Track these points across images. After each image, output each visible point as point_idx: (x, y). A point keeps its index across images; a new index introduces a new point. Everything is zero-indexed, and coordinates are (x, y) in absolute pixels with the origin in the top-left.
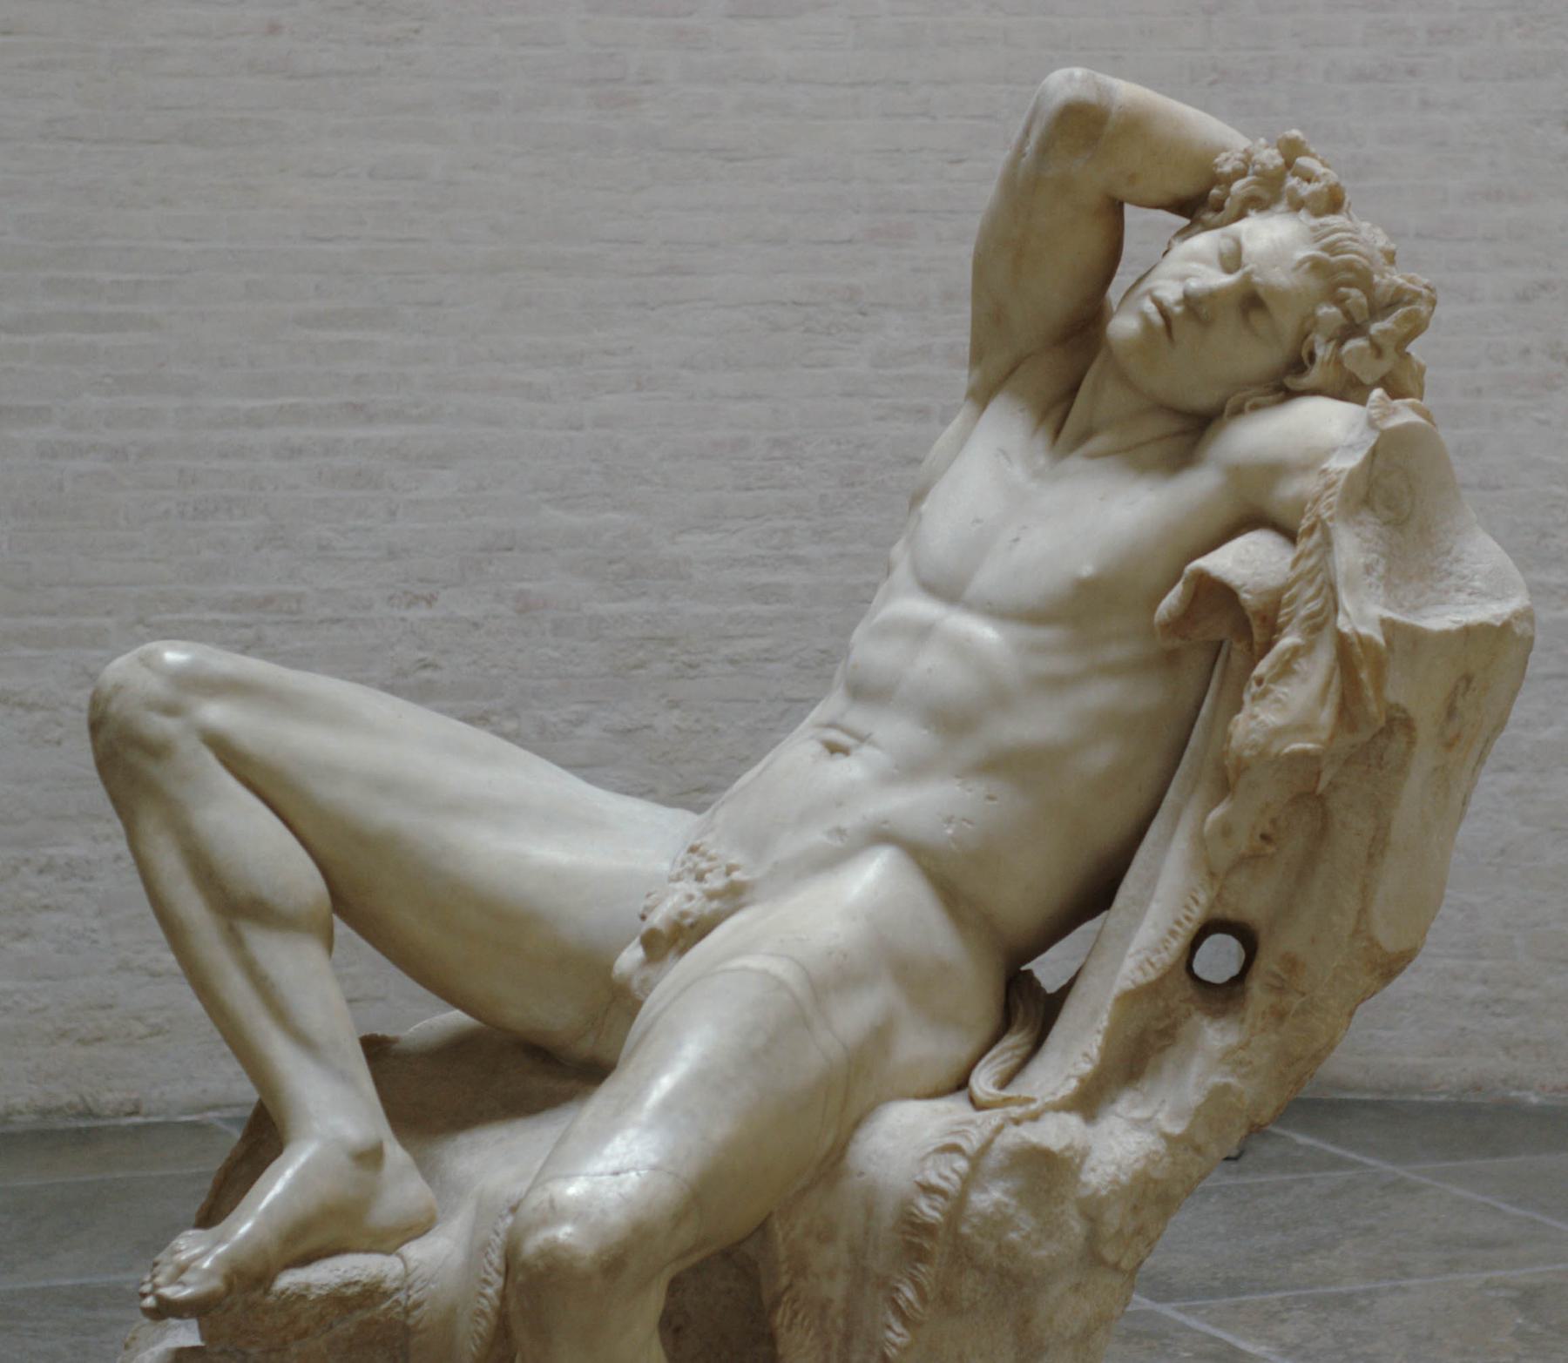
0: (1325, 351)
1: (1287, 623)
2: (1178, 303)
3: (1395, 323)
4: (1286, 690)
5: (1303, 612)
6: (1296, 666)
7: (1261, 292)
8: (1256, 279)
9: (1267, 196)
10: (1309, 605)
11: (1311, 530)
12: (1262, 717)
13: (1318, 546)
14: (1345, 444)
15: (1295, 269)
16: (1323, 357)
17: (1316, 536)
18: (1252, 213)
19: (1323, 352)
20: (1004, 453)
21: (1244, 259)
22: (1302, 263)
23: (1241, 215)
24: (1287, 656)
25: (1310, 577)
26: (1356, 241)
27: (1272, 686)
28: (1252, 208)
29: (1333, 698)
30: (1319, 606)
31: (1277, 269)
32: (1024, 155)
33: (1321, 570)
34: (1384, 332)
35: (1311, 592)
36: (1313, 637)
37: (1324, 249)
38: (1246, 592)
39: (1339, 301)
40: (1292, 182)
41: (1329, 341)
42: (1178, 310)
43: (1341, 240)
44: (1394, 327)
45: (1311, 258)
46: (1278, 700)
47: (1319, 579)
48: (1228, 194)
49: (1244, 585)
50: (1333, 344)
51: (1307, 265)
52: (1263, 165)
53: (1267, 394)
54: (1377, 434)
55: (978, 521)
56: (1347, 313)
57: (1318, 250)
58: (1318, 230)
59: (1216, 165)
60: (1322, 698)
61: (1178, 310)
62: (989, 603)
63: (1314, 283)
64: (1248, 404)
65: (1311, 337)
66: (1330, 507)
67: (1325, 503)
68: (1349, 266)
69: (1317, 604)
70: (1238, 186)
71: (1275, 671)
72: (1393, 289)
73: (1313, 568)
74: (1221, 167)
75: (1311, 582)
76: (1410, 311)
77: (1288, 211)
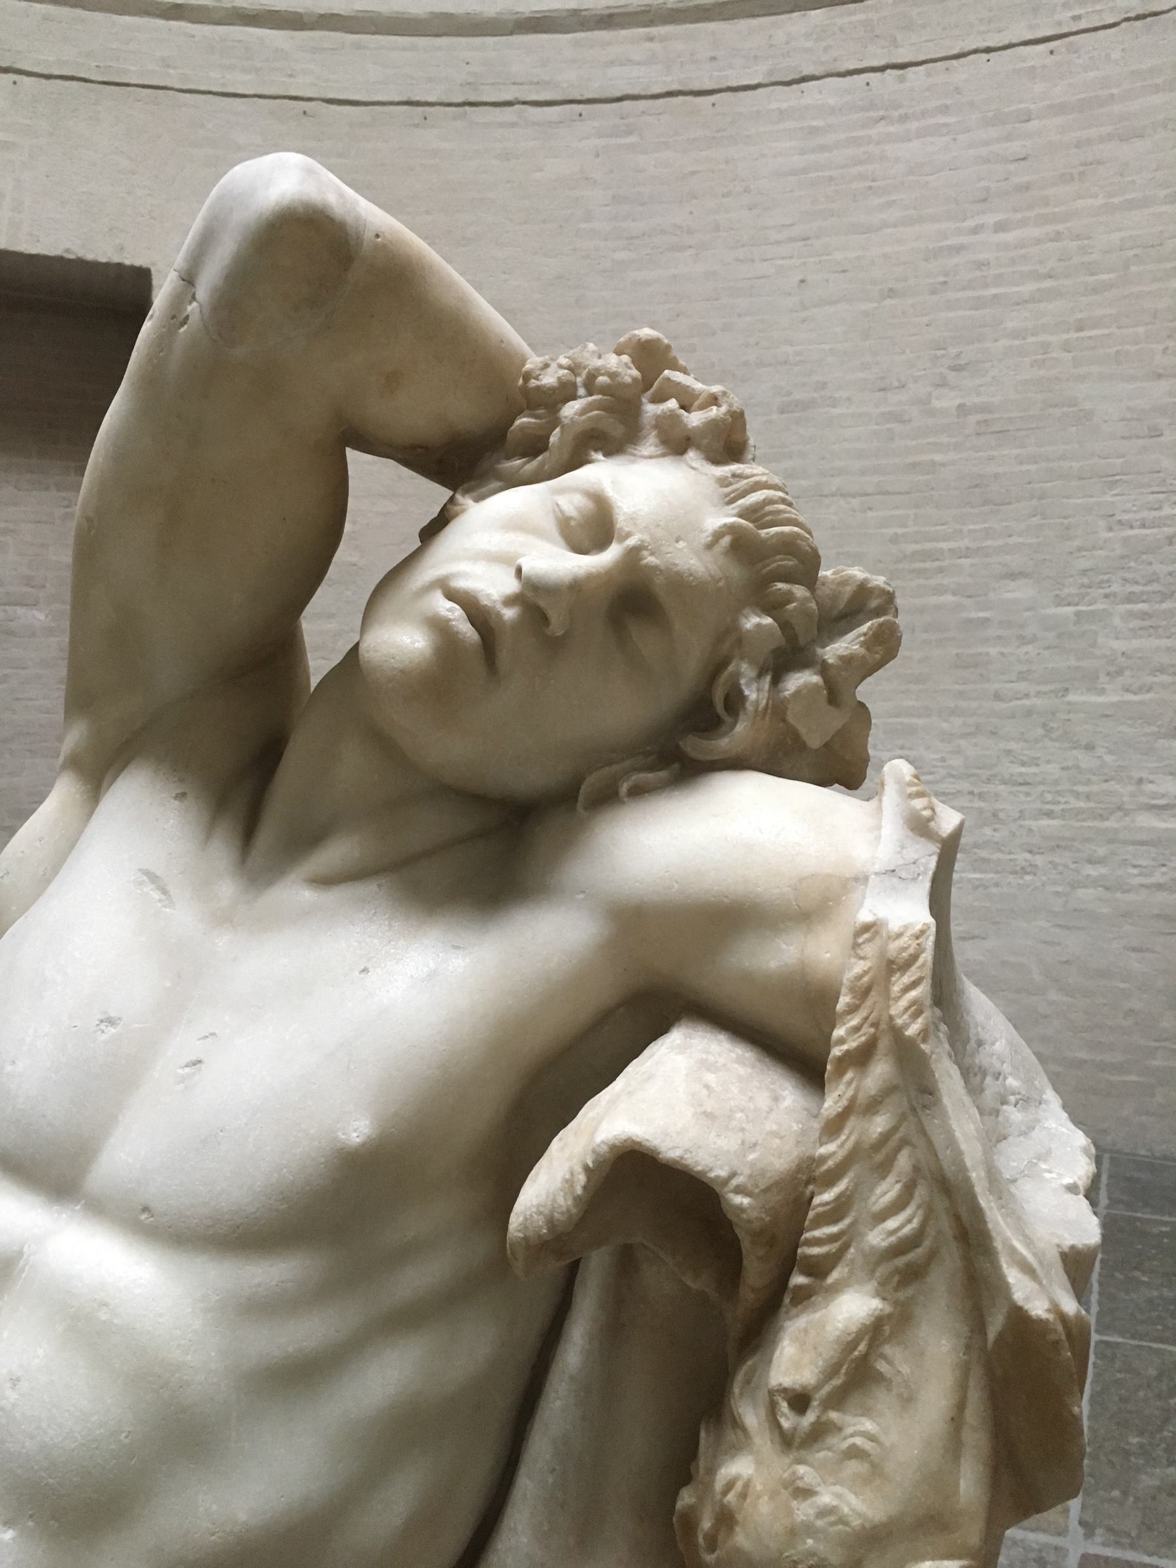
0: (758, 690)
1: (833, 1260)
2: (510, 601)
3: (862, 644)
4: (868, 1425)
5: (877, 1238)
6: (882, 1366)
7: (659, 580)
8: (650, 560)
9: (617, 430)
10: (892, 1224)
11: (862, 1057)
12: (826, 1498)
13: (888, 1091)
14: (877, 867)
15: (709, 546)
16: (757, 702)
17: (880, 1070)
18: (600, 456)
19: (755, 693)
20: (152, 877)
21: (621, 521)
22: (718, 535)
23: (576, 461)
24: (862, 1347)
25: (879, 1157)
26: (790, 505)
27: (834, 1415)
28: (596, 450)
29: (976, 1439)
30: (915, 1223)
31: (681, 544)
32: (185, 321)
33: (904, 1142)
34: (847, 661)
35: (887, 1191)
36: (902, 1295)
37: (740, 516)
38: (739, 1190)
39: (772, 607)
40: (651, 410)
41: (760, 675)
42: (509, 613)
43: (769, 501)
44: (863, 651)
45: (730, 529)
46: (854, 1453)
47: (904, 1161)
48: (555, 422)
49: (733, 1175)
50: (768, 678)
51: (726, 541)
52: (613, 375)
53: (651, 769)
54: (935, 848)
55: (111, 1022)
56: (784, 625)
57: (735, 516)
58: (730, 484)
59: (527, 377)
60: (954, 1444)
61: (509, 614)
62: (145, 1209)
63: (736, 572)
64: (624, 788)
65: (731, 668)
66: (916, 1010)
67: (904, 1002)
68: (788, 546)
69: (909, 1221)
70: (570, 410)
71: (837, 1382)
72: (849, 590)
73: (885, 1137)
74: (537, 378)
75: (884, 1169)
76: (881, 625)
77: (663, 455)
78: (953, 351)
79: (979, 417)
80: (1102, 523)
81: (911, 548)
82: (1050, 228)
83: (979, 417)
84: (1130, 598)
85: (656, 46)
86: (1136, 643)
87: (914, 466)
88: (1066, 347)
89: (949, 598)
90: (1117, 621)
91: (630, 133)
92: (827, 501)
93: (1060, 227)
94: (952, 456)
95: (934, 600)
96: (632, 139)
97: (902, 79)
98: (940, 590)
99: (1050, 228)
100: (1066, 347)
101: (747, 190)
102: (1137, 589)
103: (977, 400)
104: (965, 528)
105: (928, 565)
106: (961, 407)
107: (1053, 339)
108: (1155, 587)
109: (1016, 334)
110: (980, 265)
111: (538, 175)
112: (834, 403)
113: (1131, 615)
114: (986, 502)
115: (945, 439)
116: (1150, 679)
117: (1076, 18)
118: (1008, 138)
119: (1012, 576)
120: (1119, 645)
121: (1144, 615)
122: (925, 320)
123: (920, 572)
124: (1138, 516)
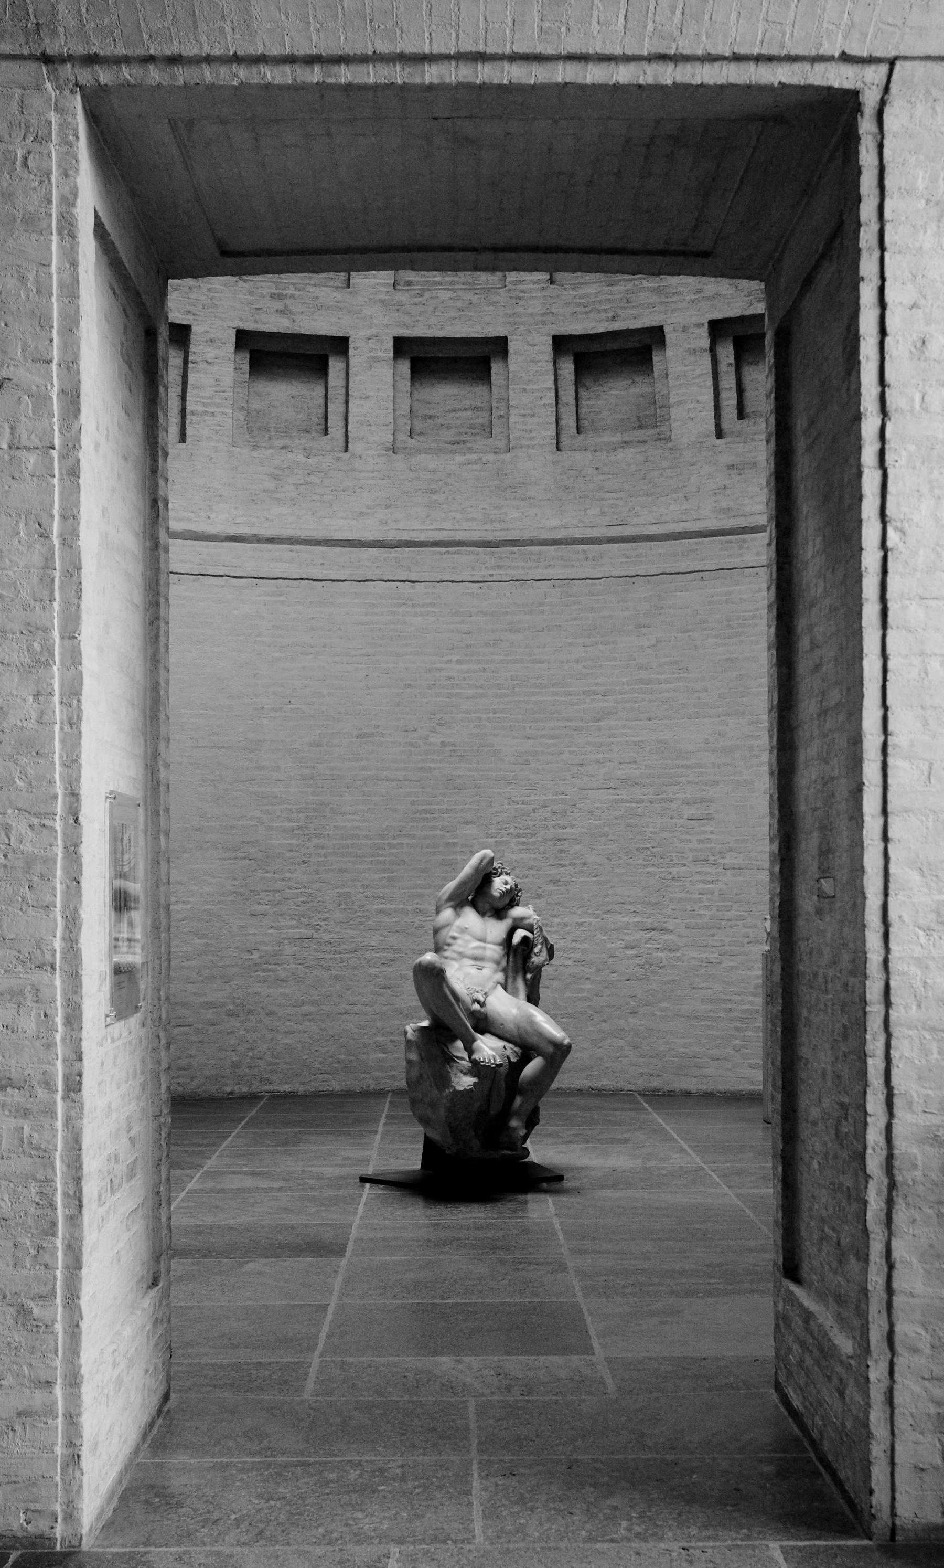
78: (438, 716)
79: (451, 748)
80: (506, 801)
81: (420, 808)
82: (480, 666)
83: (451, 748)
84: (518, 836)
85: (294, 554)
86: (521, 856)
87: (422, 768)
88: (489, 720)
89: (438, 832)
90: (513, 845)
91: (281, 595)
92: (380, 783)
93: (486, 666)
94: (439, 765)
95: (431, 833)
96: (282, 598)
97: (413, 588)
98: (433, 828)
99: (480, 666)
100: (489, 720)
101: (340, 629)
102: (521, 831)
103: (451, 740)
104: (446, 800)
105: (428, 816)
106: (442, 742)
107: (484, 716)
108: (528, 831)
109: (468, 712)
110: (450, 678)
111: (236, 612)
112: (383, 735)
113: (519, 843)
114: (455, 788)
115: (435, 757)
116: (527, 872)
117: (491, 575)
118: (462, 622)
119: (467, 823)
120: (514, 857)
121: (524, 843)
122: (426, 700)
123: (424, 819)
124: (521, 799)
